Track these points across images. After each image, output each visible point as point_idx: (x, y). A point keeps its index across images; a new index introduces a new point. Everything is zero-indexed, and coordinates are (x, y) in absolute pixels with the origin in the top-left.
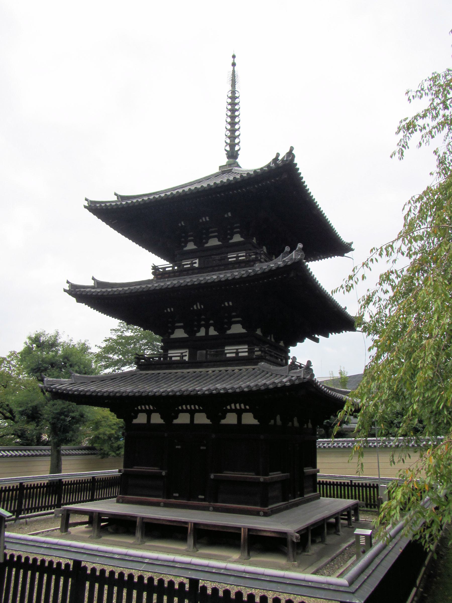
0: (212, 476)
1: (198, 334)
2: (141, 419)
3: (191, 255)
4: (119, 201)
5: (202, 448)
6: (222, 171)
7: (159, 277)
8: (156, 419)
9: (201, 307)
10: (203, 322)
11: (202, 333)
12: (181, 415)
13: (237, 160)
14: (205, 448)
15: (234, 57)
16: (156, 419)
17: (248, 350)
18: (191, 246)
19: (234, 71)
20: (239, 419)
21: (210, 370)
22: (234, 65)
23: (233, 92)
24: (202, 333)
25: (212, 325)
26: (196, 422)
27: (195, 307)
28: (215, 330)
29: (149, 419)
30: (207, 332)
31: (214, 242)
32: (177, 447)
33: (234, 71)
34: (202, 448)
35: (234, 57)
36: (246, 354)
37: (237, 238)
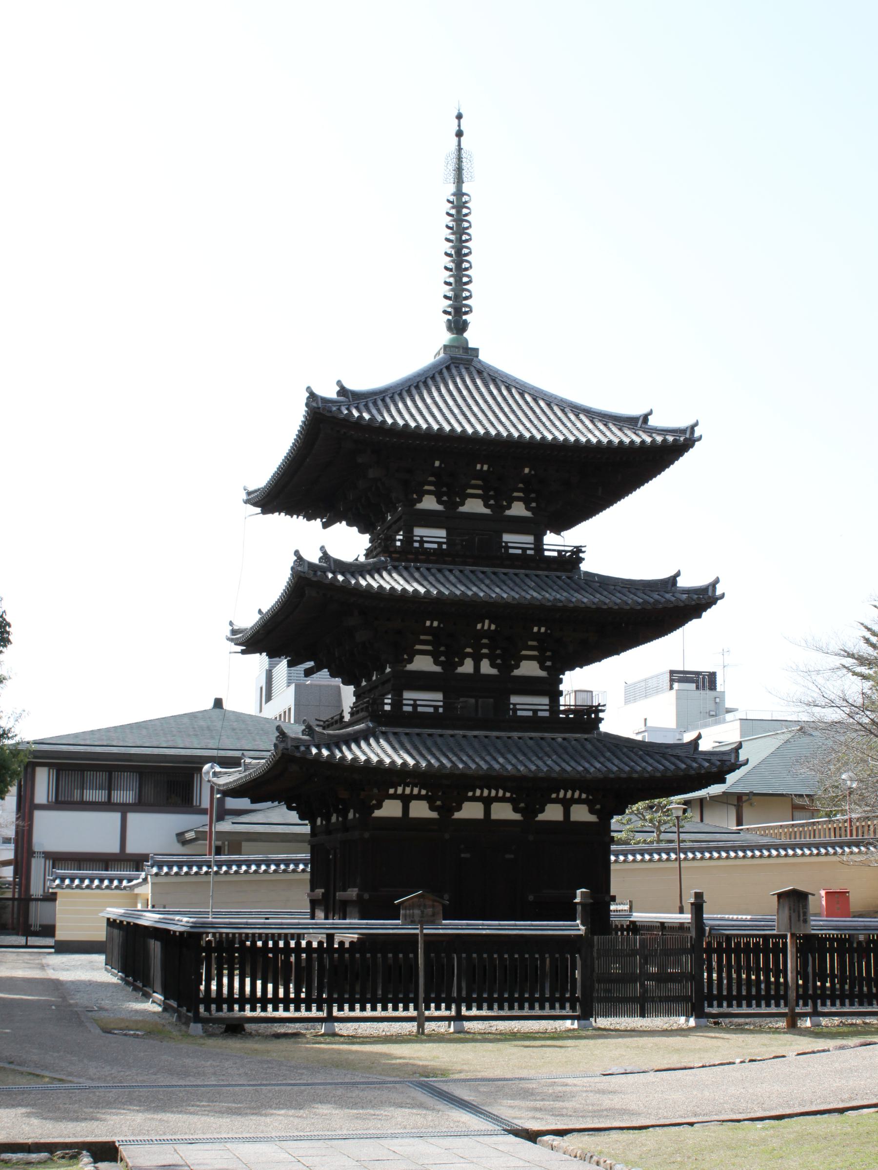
0: (531, 898)
1: (460, 670)
2: (391, 809)
3: (429, 519)
4: (350, 402)
5: (508, 856)
6: (452, 358)
7: (393, 555)
8: (420, 810)
9: (490, 626)
10: (469, 650)
11: (468, 667)
12: (467, 805)
13: (466, 335)
14: (512, 856)
15: (459, 117)
16: (420, 810)
17: (550, 707)
18: (429, 503)
19: (460, 149)
20: (567, 813)
21: (515, 735)
22: (459, 134)
23: (459, 194)
24: (468, 667)
25: (485, 656)
26: (494, 816)
27: (479, 626)
28: (493, 665)
29: (406, 809)
30: (477, 667)
31: (474, 506)
32: (463, 855)
33: (460, 149)
34: (508, 856)
35: (459, 117)
36: (547, 714)
37: (518, 510)
